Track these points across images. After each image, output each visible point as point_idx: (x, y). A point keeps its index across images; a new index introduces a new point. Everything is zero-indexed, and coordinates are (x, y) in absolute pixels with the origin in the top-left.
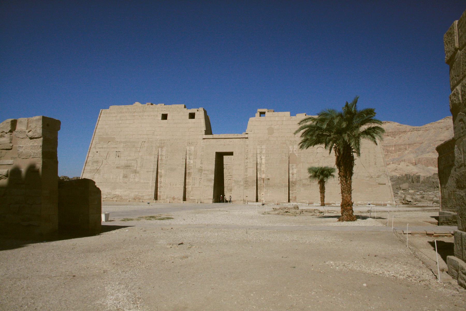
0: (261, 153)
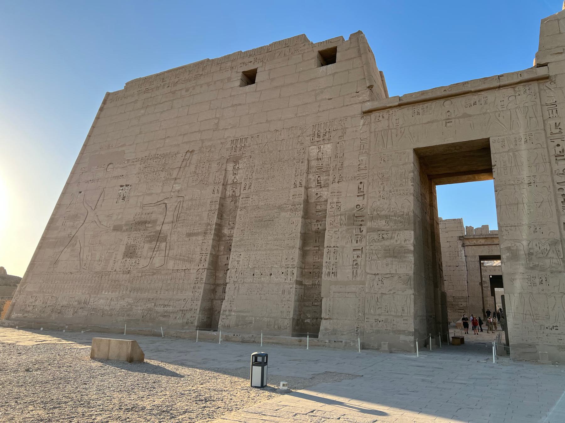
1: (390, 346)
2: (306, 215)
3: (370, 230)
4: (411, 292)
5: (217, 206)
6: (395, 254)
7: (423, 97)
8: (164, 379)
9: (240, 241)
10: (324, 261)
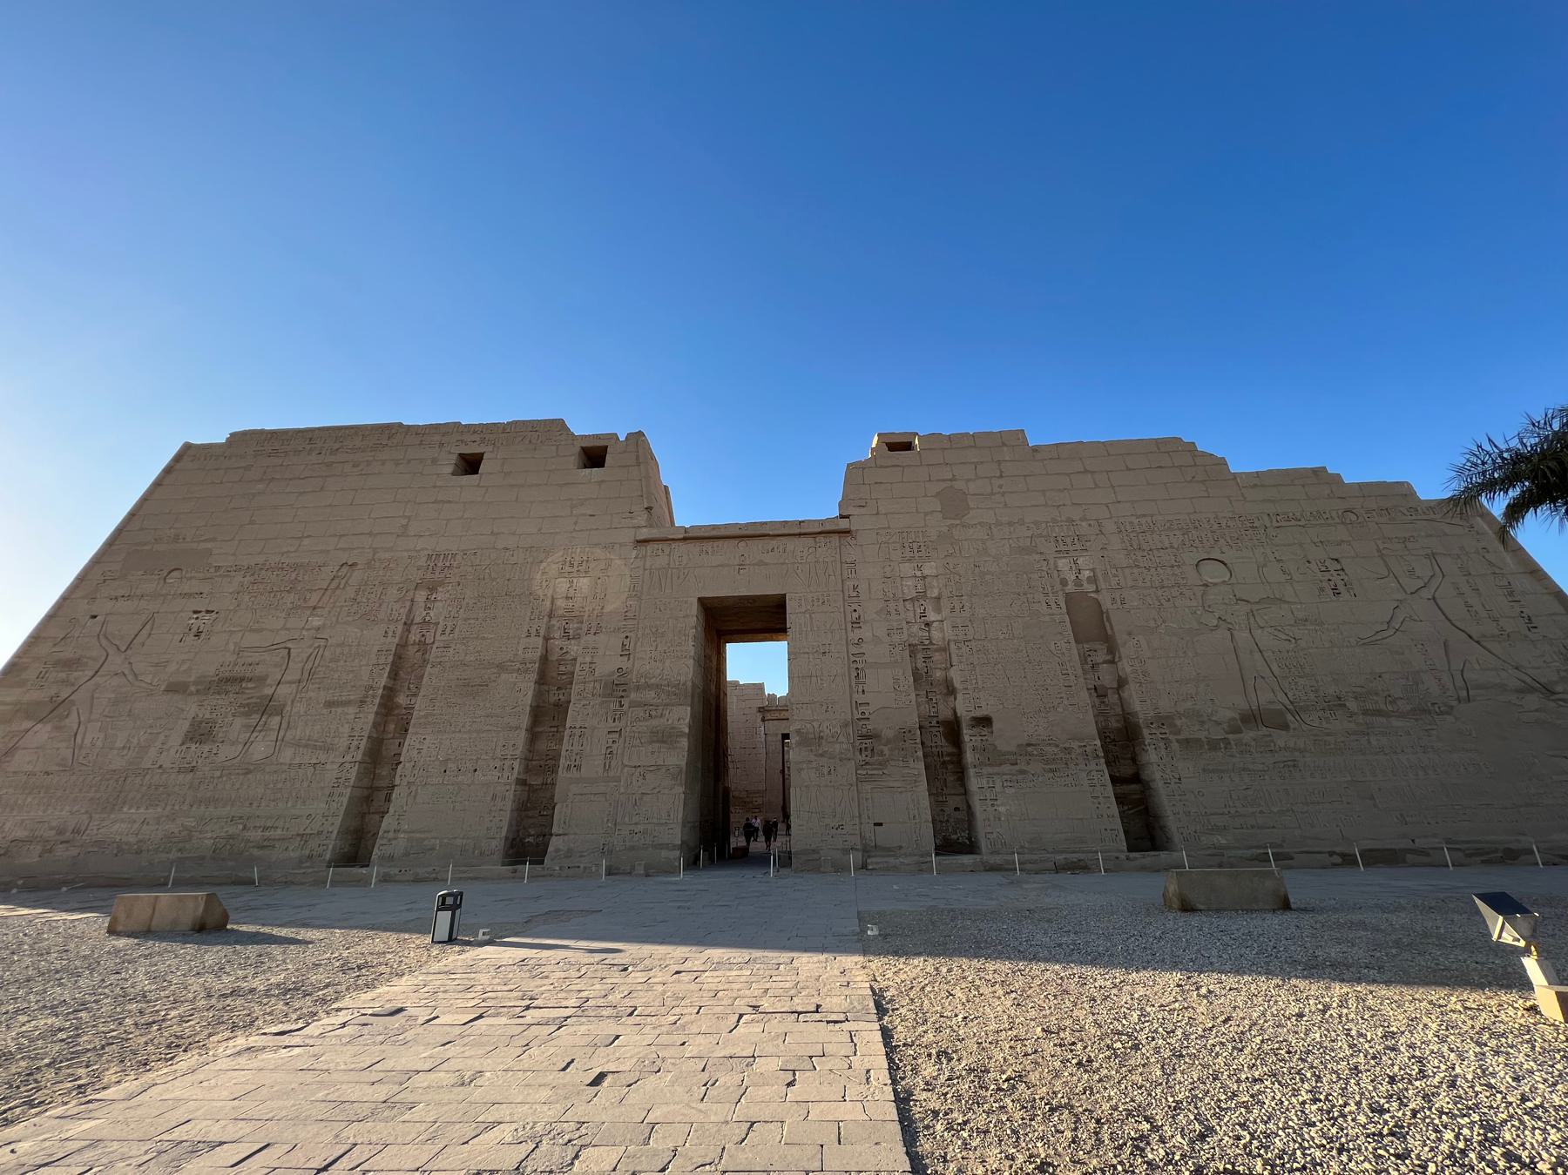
0: (922, 596)
1: (647, 867)
2: (542, 680)
3: (633, 705)
4: (682, 789)
5: (390, 659)
6: (664, 738)
7: (714, 533)
8: (276, 950)
9: (426, 716)
10: (564, 749)
